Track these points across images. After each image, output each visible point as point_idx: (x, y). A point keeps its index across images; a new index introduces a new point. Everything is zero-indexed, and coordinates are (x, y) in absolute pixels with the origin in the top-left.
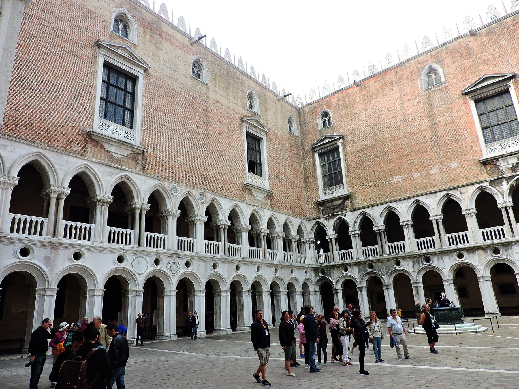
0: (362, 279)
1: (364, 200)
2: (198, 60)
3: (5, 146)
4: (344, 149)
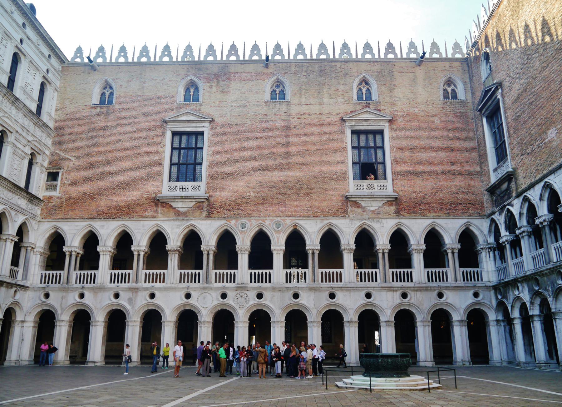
0: (532, 303)
1: (525, 178)
2: (278, 79)
3: (103, 226)
4: (504, 103)
